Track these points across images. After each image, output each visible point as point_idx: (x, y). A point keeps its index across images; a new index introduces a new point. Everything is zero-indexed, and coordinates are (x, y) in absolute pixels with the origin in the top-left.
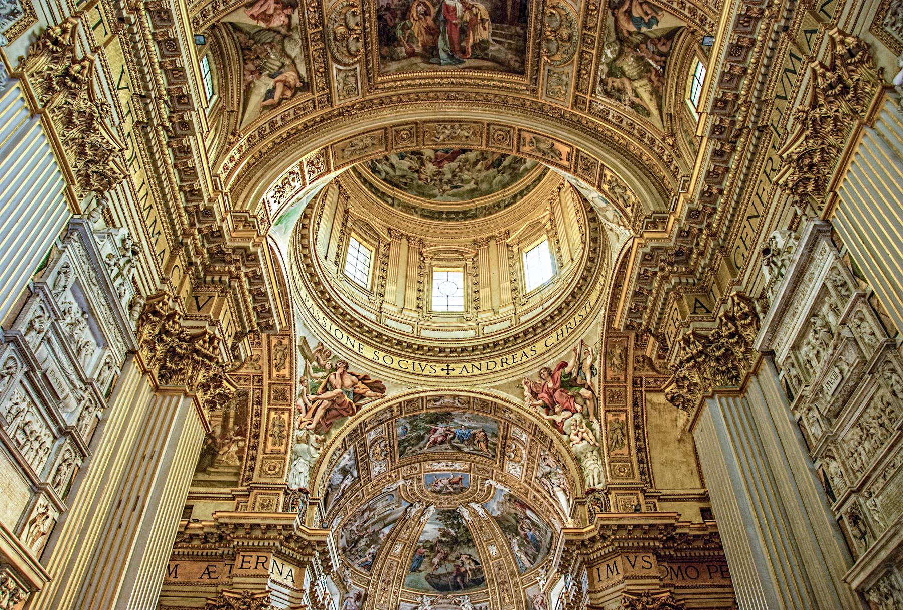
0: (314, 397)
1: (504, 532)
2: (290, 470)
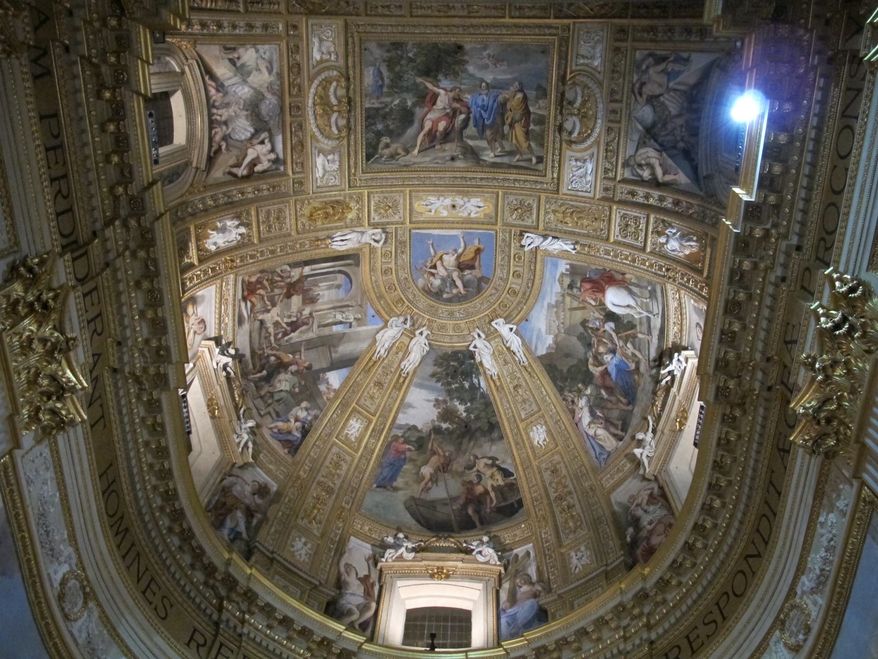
1: (561, 390)
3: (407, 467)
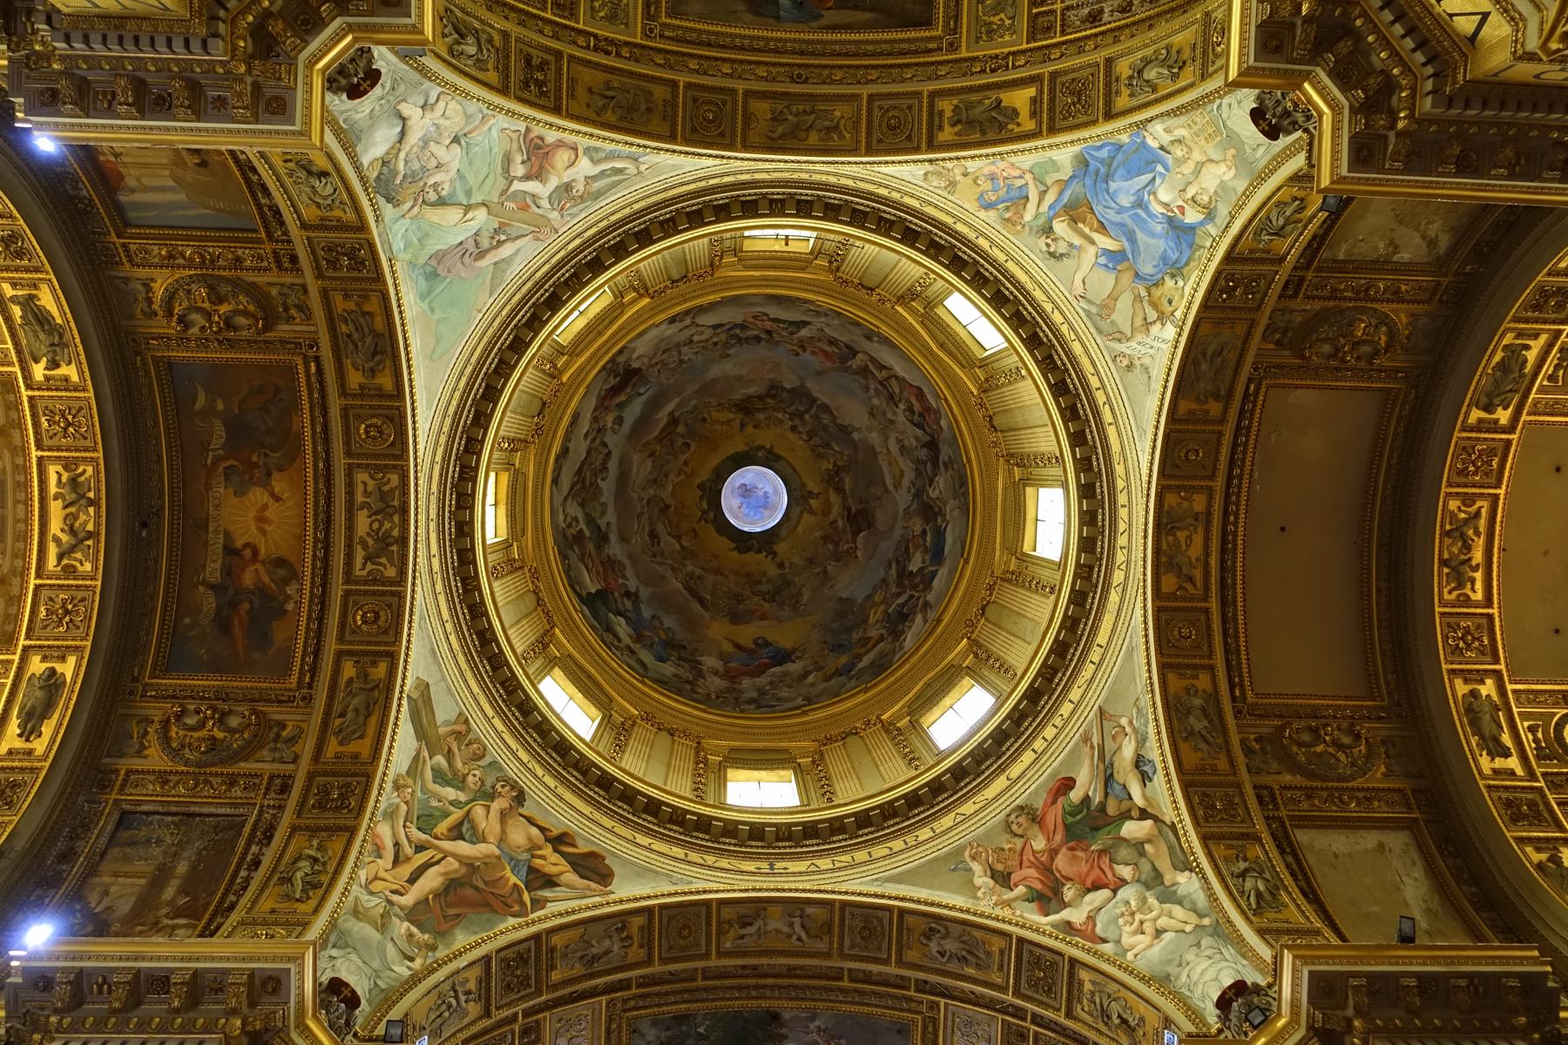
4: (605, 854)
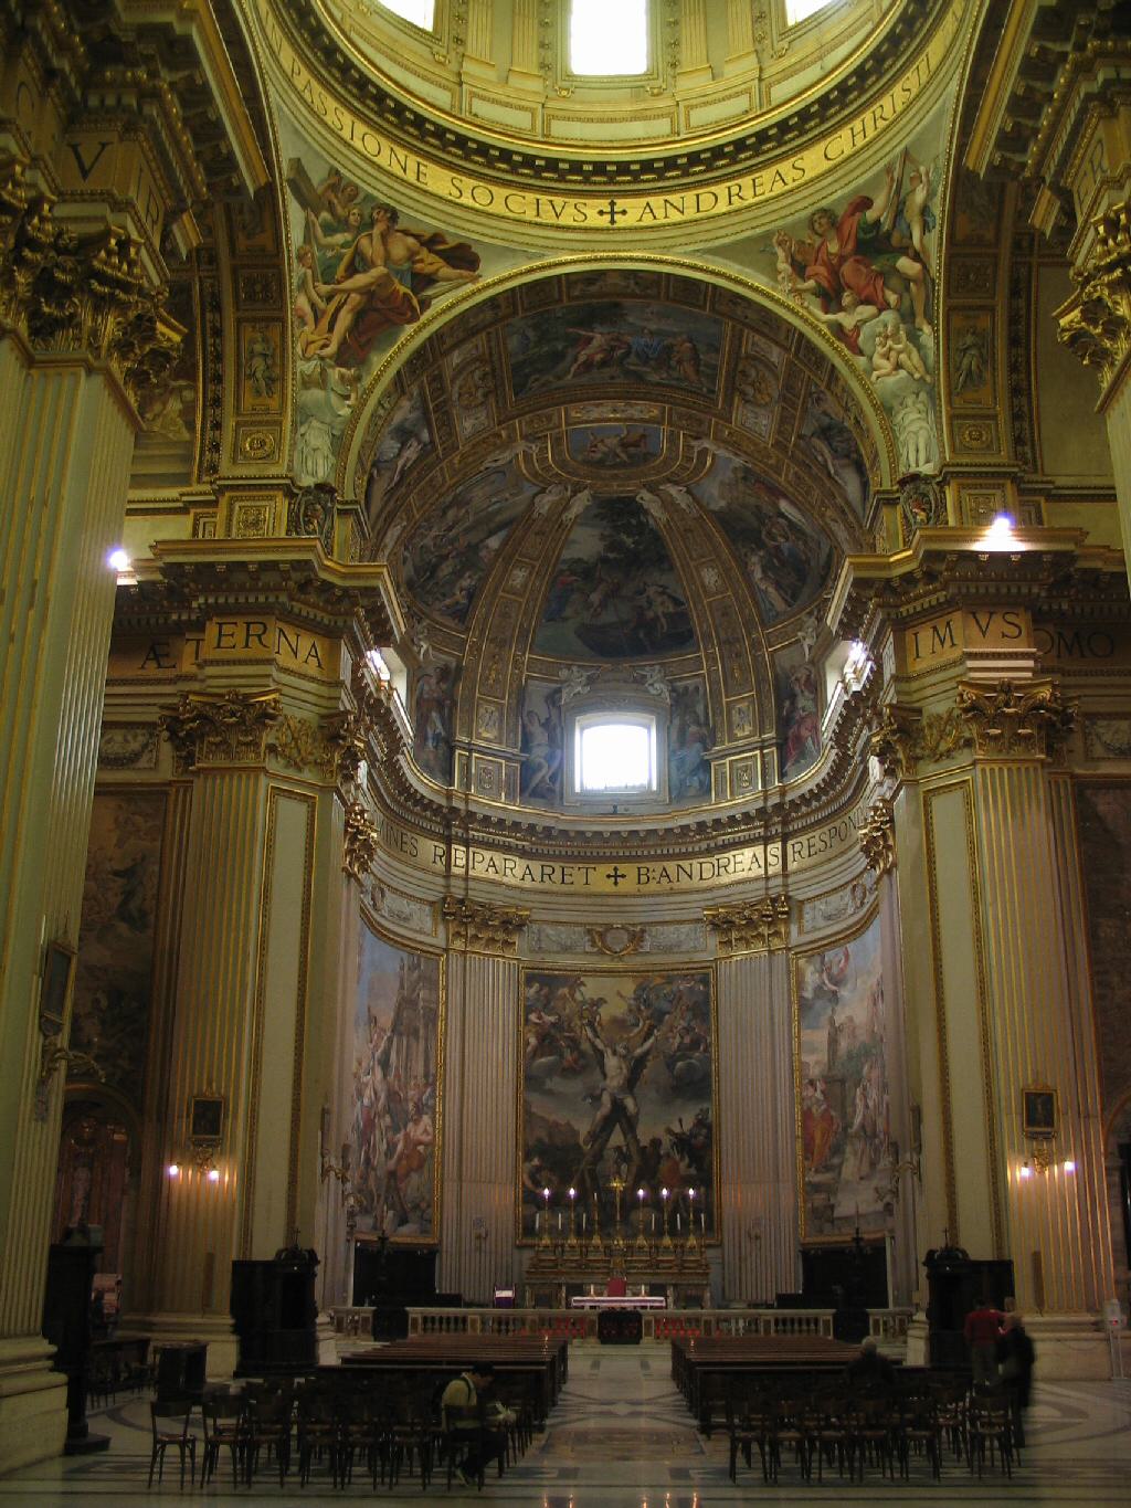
0: (328, 288)
2: (293, 445)
3: (575, 596)
4: (468, 242)
